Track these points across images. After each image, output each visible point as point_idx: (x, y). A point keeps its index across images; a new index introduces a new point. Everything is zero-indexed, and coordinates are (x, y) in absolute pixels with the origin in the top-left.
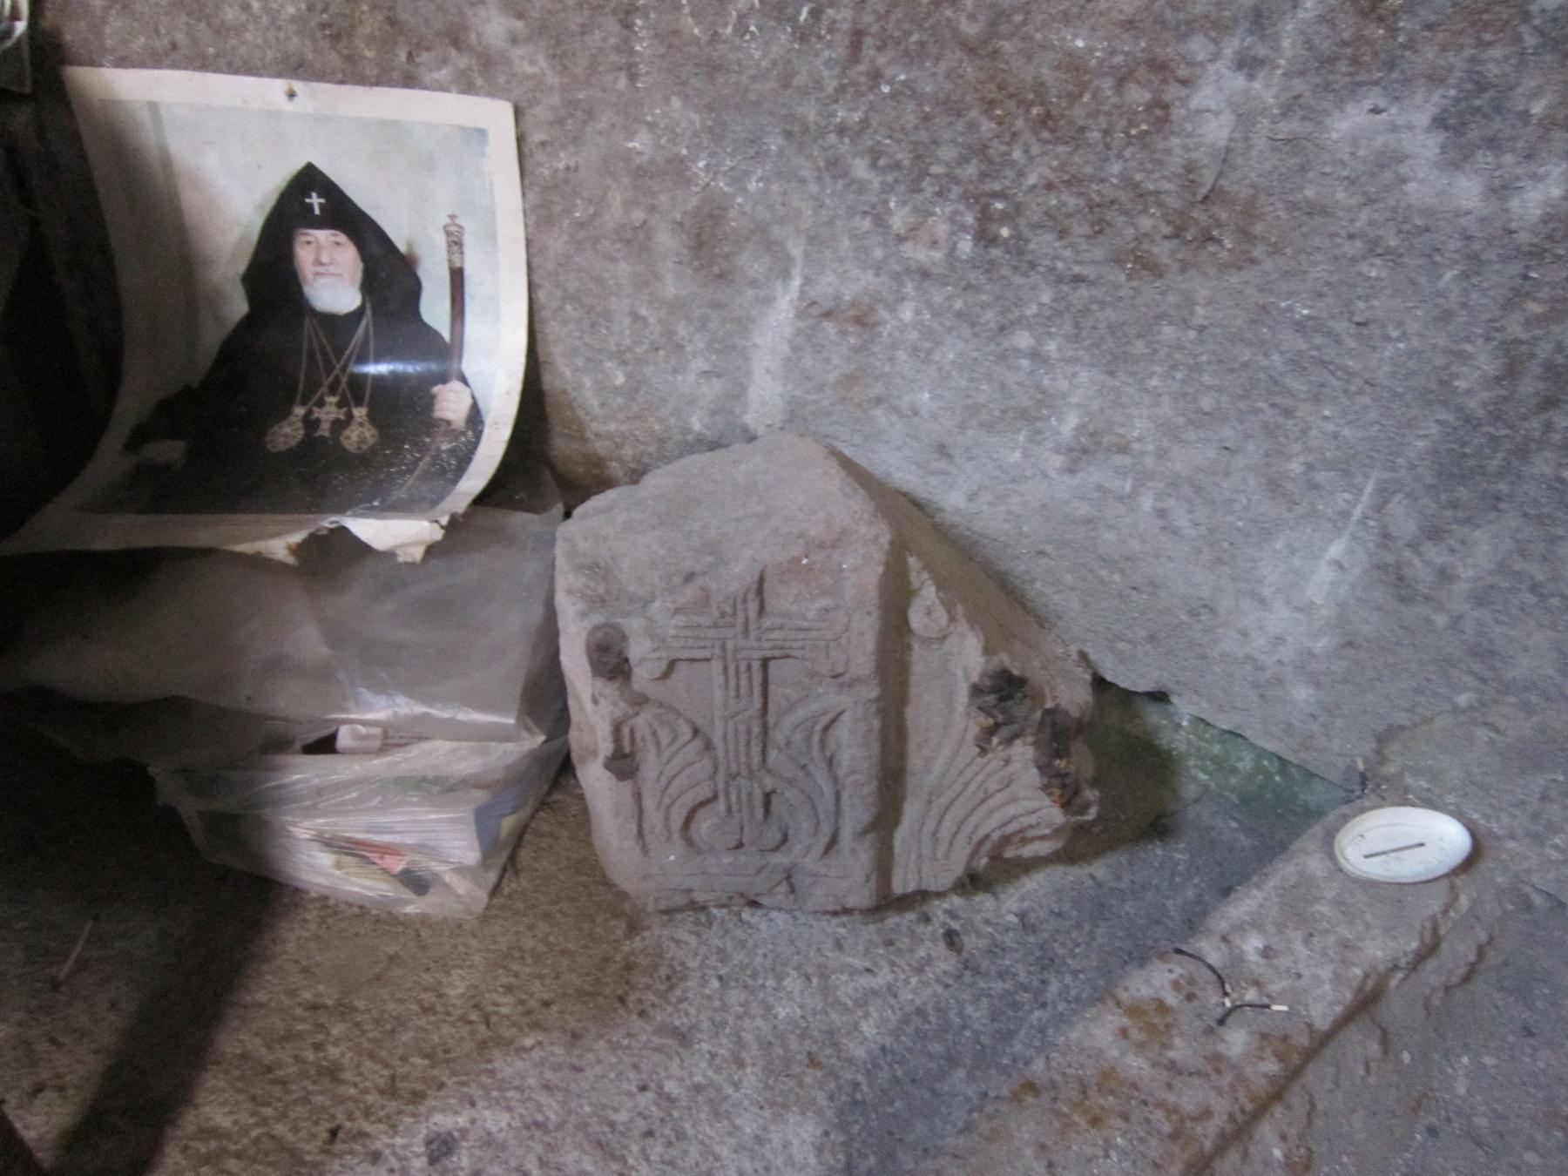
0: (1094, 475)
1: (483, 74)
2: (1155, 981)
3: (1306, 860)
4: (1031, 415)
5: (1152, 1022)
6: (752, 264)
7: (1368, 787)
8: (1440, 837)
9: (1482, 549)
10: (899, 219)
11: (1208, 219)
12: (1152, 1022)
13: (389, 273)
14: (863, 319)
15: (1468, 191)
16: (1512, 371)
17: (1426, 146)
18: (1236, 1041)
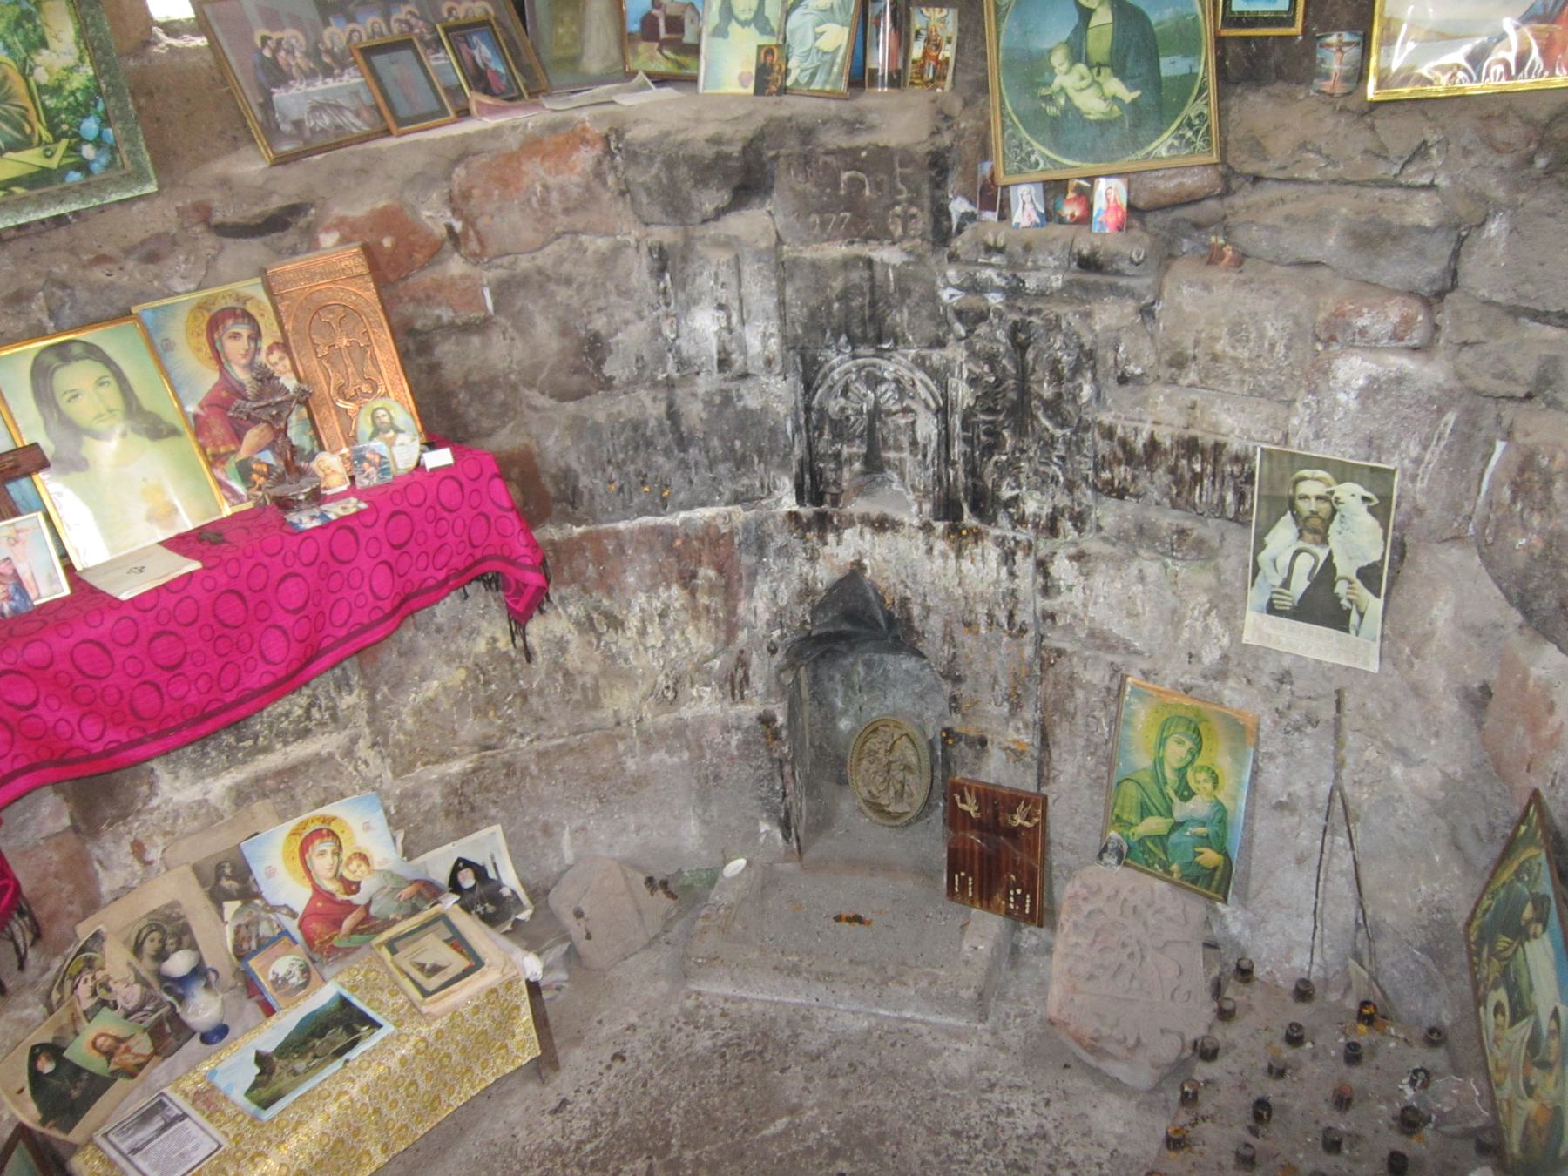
0: (642, 833)
1: (492, 821)
2: (704, 912)
3: (720, 880)
4: (624, 830)
5: (706, 917)
6: (557, 829)
7: (725, 862)
8: (741, 863)
9: (714, 810)
10: (583, 806)
11: (640, 781)
12: (706, 917)
13: (480, 872)
14: (583, 829)
15: (676, 759)
16: (698, 779)
17: (666, 757)
18: (721, 911)
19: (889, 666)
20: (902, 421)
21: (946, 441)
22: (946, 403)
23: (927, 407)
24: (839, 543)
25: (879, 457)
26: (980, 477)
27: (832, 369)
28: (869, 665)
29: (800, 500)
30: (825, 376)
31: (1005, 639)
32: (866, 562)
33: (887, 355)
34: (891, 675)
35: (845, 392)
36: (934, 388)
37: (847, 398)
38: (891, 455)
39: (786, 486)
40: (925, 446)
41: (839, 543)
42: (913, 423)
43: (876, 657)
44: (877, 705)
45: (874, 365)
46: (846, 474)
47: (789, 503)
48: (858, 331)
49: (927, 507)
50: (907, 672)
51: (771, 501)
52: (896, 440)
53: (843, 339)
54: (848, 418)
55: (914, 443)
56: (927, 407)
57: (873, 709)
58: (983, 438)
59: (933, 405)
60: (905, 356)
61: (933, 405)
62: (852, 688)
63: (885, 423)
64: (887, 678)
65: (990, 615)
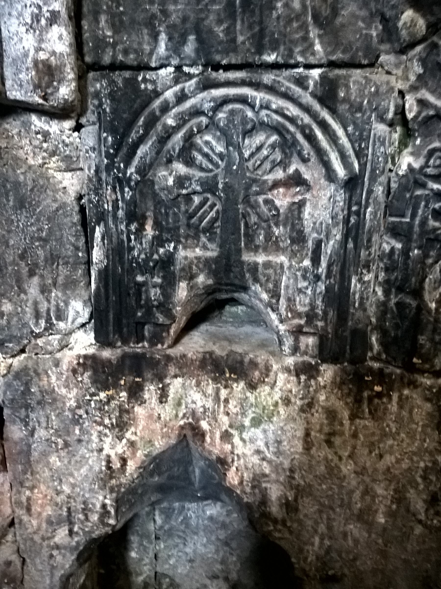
19: (190, 513)
20: (282, 200)
21: (354, 231)
22: (363, 166)
23: (330, 175)
24: (163, 397)
25: (242, 263)
26: (418, 293)
27: (165, 108)
28: (168, 514)
29: (102, 340)
30: (153, 121)
31: (418, 530)
32: (204, 425)
33: (268, 78)
34: (193, 522)
35: (186, 154)
36: (344, 140)
37: (189, 162)
38: (261, 259)
39: (79, 309)
40: (318, 244)
41: (163, 397)
42: (301, 204)
43: (177, 505)
44: (174, 552)
45: (243, 100)
46: (182, 291)
47: (84, 342)
48: (220, 31)
49: (310, 341)
50: (211, 518)
51: (55, 339)
52: (269, 236)
53: (190, 48)
54: (188, 198)
55: (299, 238)
56: (330, 175)
57: (169, 557)
58: (432, 223)
59: (341, 172)
60: (301, 82)
61: (341, 172)
62: (148, 537)
63: (255, 206)
64: (188, 526)
65: (400, 498)
